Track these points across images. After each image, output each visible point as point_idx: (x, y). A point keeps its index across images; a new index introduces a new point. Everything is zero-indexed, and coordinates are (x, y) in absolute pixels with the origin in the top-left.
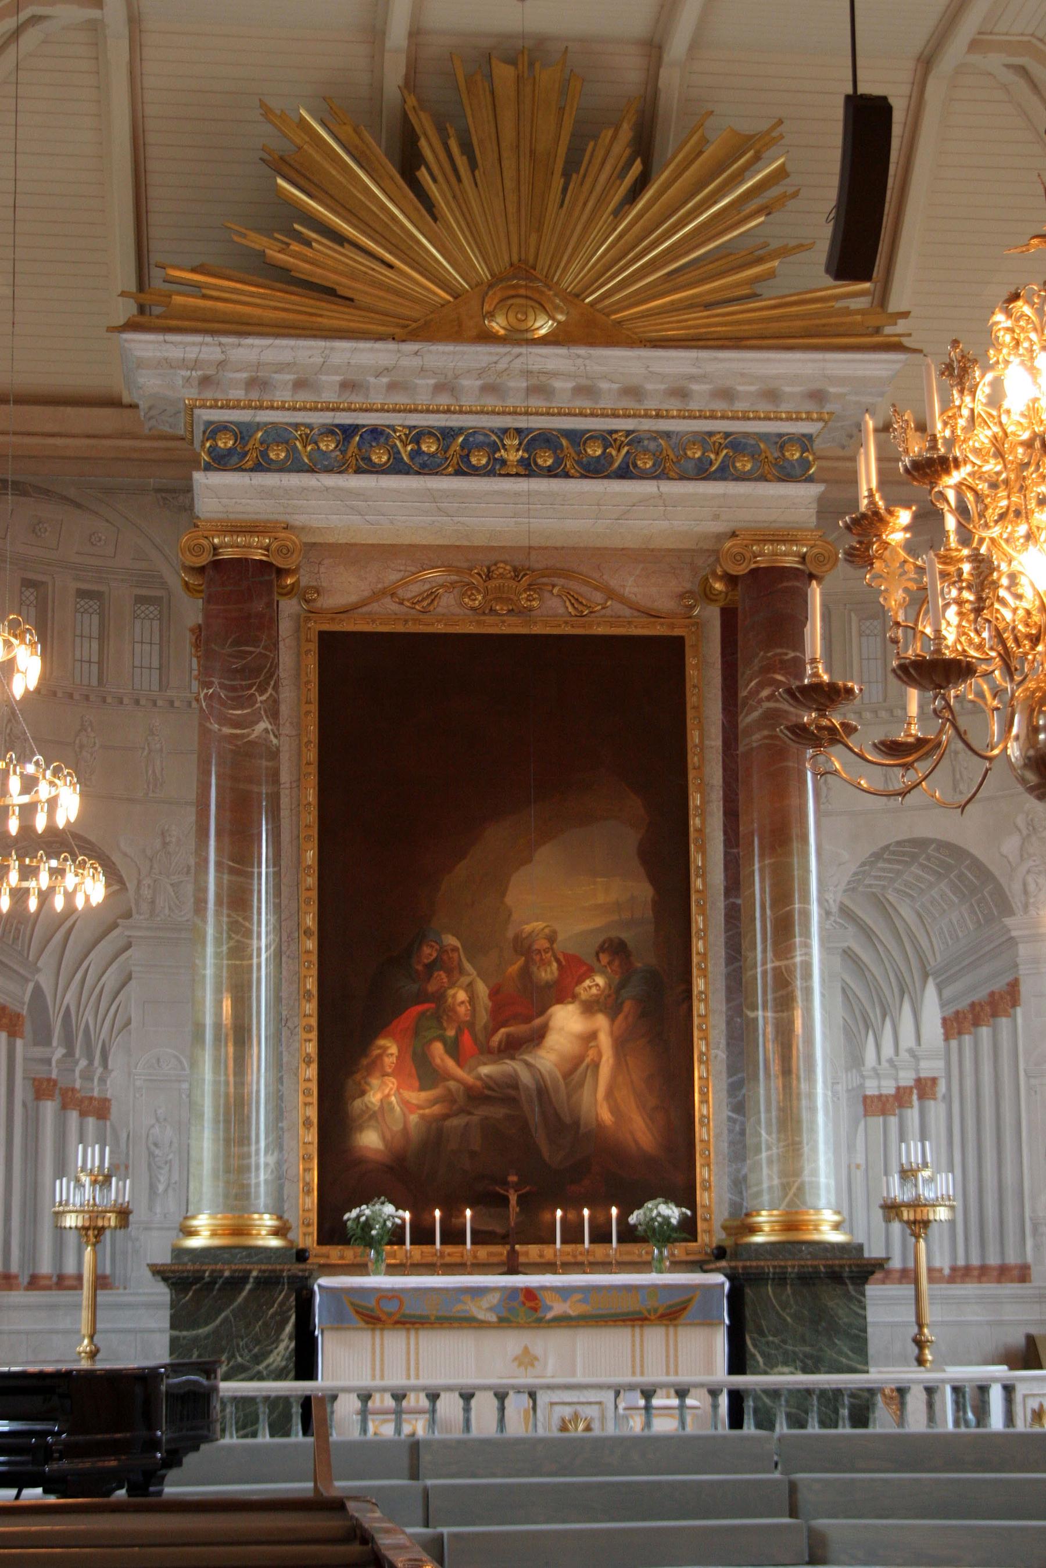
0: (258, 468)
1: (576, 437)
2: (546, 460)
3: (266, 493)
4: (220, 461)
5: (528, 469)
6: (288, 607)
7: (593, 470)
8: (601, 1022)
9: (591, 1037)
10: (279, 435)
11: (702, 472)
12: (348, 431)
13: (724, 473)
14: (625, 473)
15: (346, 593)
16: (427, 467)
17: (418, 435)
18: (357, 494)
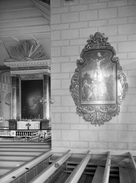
0: (14, 70)
1: (33, 67)
2: (31, 69)
3: (14, 72)
4: (12, 70)
5: (30, 69)
6: (20, 79)
7: (34, 69)
8: (38, 105)
9: (37, 106)
10: (15, 68)
11: (41, 69)
12: (19, 68)
13: (42, 69)
14: (36, 69)
15: (23, 78)
16: (24, 70)
17: (23, 67)
18: (20, 72)
